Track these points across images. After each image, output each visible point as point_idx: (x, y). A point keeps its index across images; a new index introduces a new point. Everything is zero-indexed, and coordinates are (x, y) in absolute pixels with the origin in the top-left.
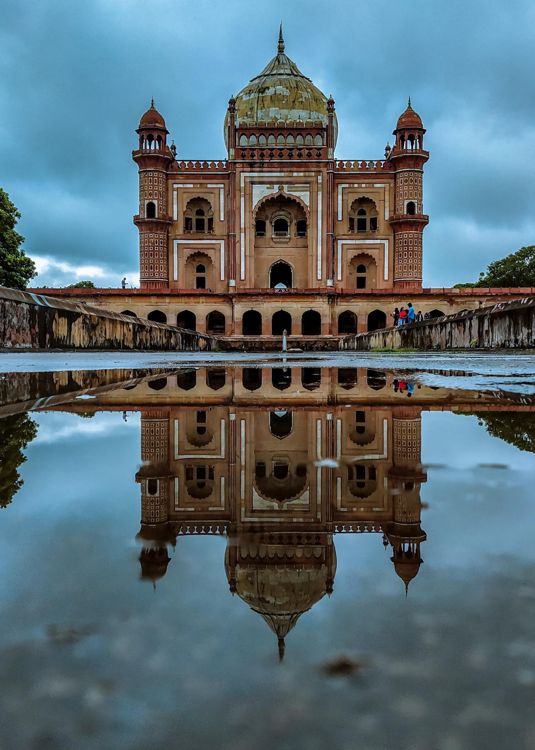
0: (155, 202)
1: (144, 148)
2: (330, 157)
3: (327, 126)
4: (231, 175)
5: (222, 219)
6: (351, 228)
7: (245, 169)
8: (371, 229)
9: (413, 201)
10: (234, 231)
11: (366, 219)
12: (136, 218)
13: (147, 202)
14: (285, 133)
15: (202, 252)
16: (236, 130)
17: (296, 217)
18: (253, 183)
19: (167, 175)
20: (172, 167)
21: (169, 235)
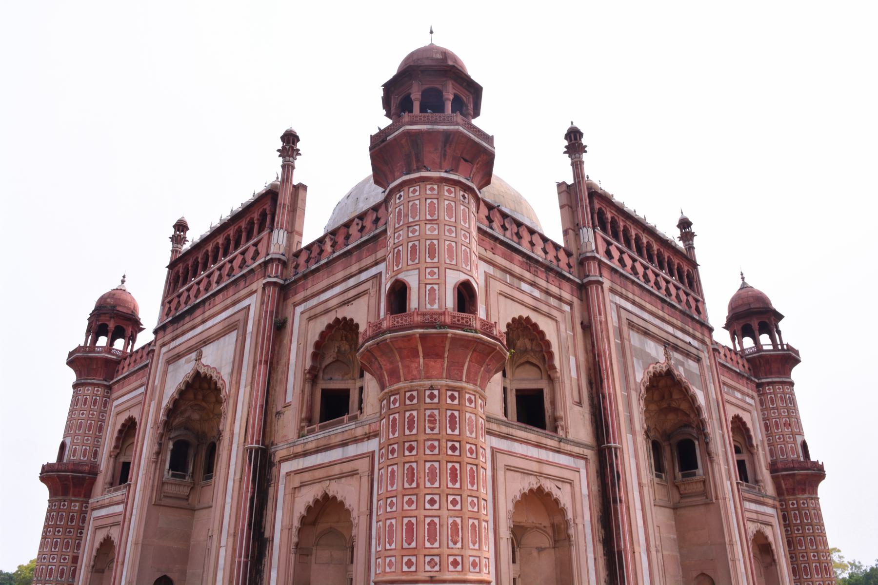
0: (68, 441)
9: (401, 276)
18: (169, 362)
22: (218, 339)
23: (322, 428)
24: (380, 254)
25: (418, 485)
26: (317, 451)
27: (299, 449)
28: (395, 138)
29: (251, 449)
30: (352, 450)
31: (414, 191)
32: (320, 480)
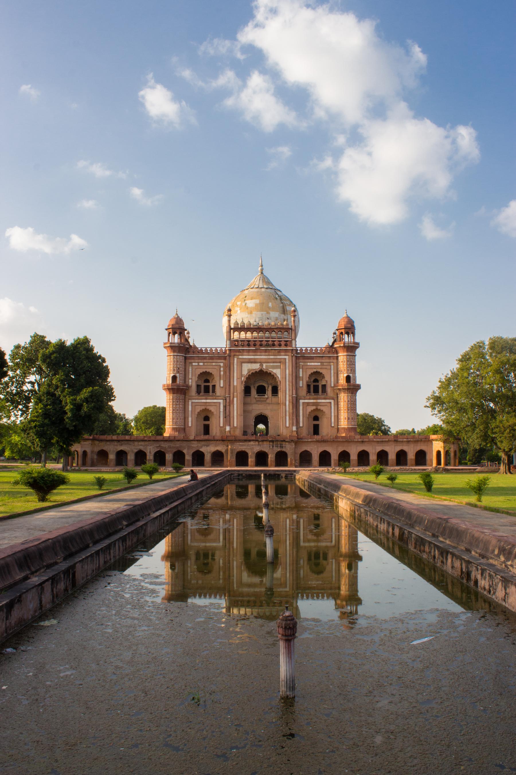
0: (178, 375)
1: (171, 341)
2: (294, 346)
5: (222, 385)
6: (309, 391)
8: (322, 392)
10: (229, 394)
12: (164, 386)
13: (172, 375)
16: (231, 329)
17: (271, 384)
18: (242, 363)
19: (186, 358)
20: (189, 352)
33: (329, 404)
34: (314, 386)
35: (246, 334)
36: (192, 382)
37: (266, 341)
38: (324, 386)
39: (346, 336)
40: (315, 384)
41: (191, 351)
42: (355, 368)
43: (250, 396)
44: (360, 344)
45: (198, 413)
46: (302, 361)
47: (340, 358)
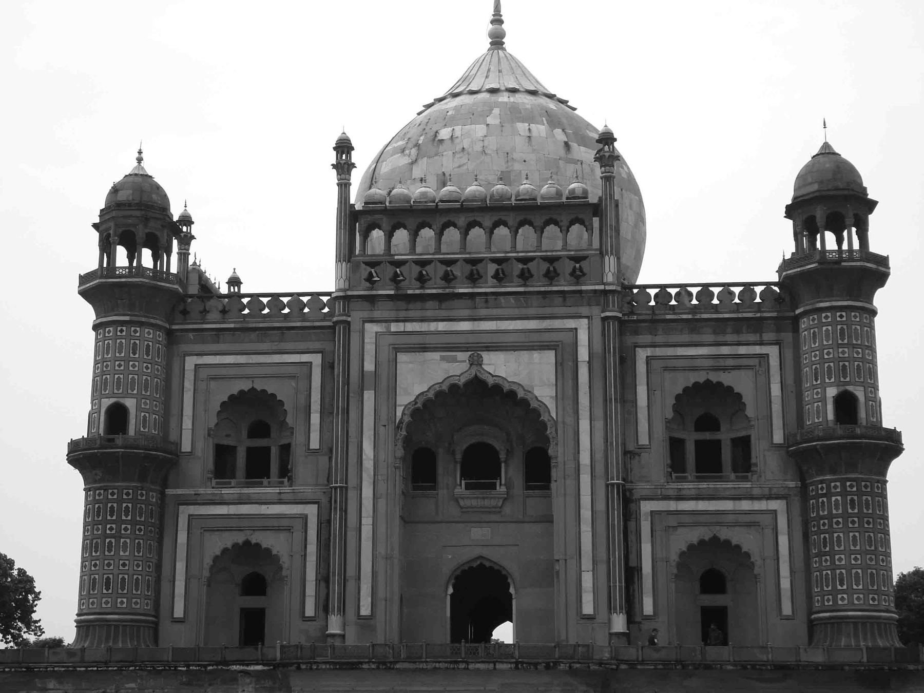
0: (130, 403)
2: (610, 278)
3: (600, 199)
4: (340, 329)
5: (315, 444)
6: (677, 465)
7: (377, 314)
8: (735, 470)
9: (850, 388)
11: (719, 442)
13: (107, 403)
14: (487, 222)
15: (254, 541)
18: (397, 349)
19: (170, 333)
20: (185, 312)
21: (169, 491)
22: (515, 350)
23: (699, 479)
24: (767, 337)
25: (876, 548)
26: (697, 498)
27: (671, 493)
28: (852, 268)
29: (618, 485)
30: (745, 505)
31: (855, 317)
32: (705, 524)
33: (768, 519)
34: (698, 443)
35: (414, 235)
36: (191, 433)
37: (494, 260)
38: (743, 445)
39: (830, 237)
40: (707, 436)
41: (195, 307)
42: (873, 362)
43: (434, 488)
44: (891, 264)
45: (216, 559)
46: (646, 338)
47: (804, 324)
